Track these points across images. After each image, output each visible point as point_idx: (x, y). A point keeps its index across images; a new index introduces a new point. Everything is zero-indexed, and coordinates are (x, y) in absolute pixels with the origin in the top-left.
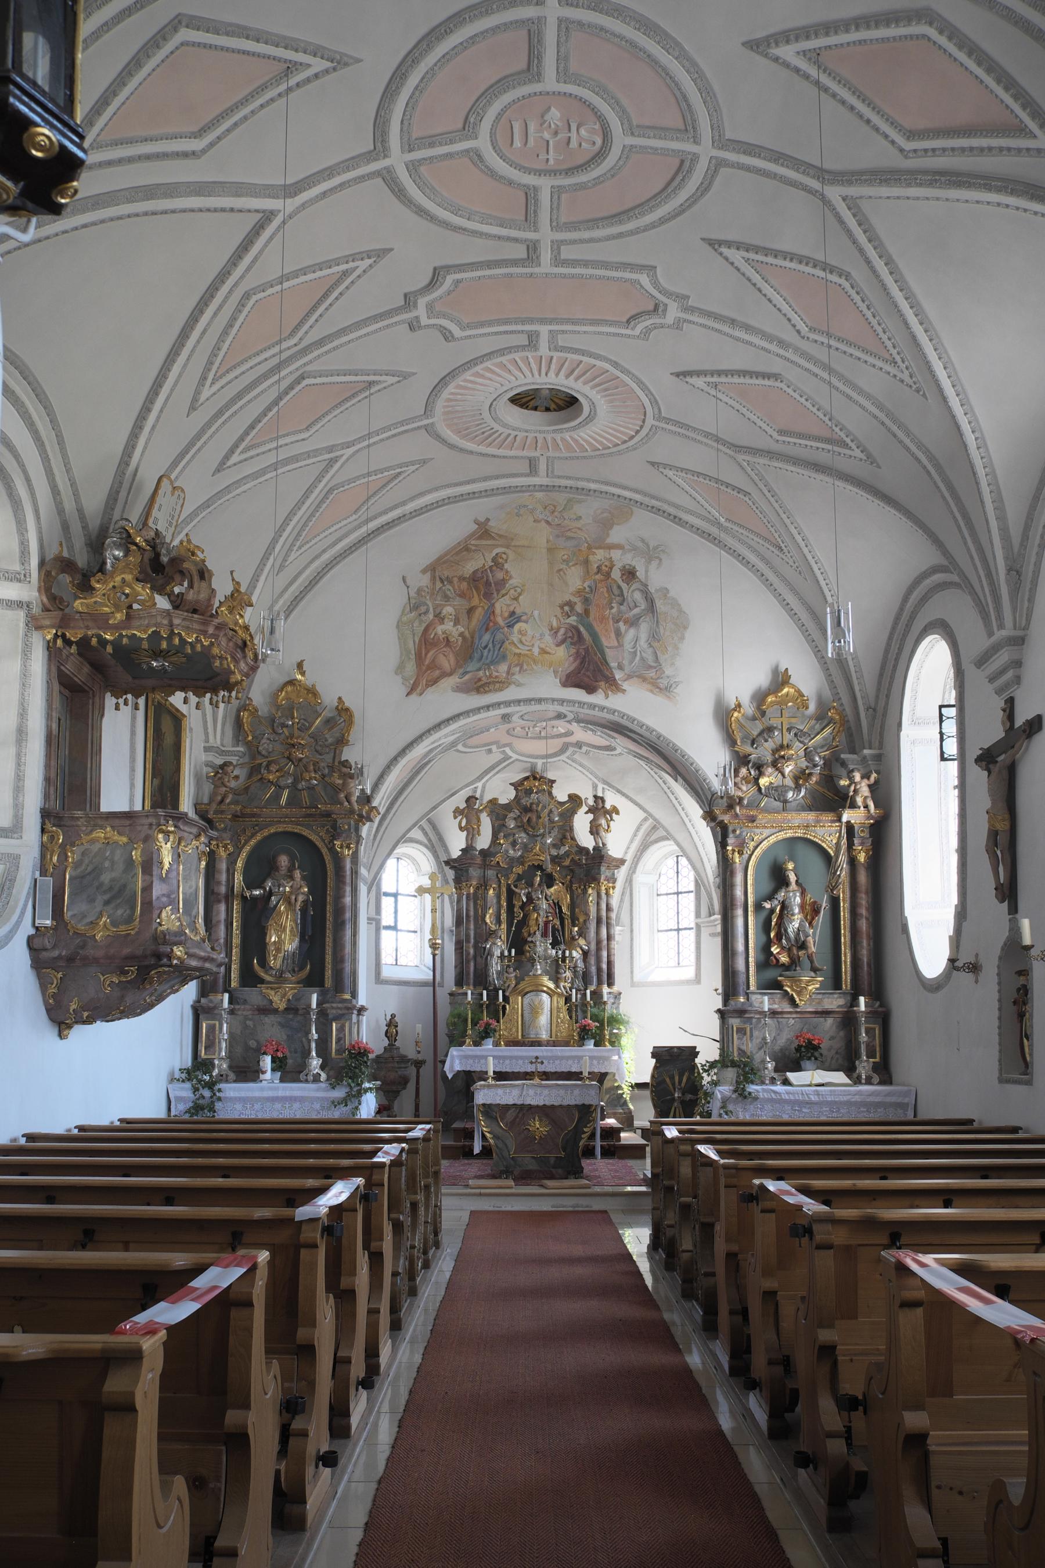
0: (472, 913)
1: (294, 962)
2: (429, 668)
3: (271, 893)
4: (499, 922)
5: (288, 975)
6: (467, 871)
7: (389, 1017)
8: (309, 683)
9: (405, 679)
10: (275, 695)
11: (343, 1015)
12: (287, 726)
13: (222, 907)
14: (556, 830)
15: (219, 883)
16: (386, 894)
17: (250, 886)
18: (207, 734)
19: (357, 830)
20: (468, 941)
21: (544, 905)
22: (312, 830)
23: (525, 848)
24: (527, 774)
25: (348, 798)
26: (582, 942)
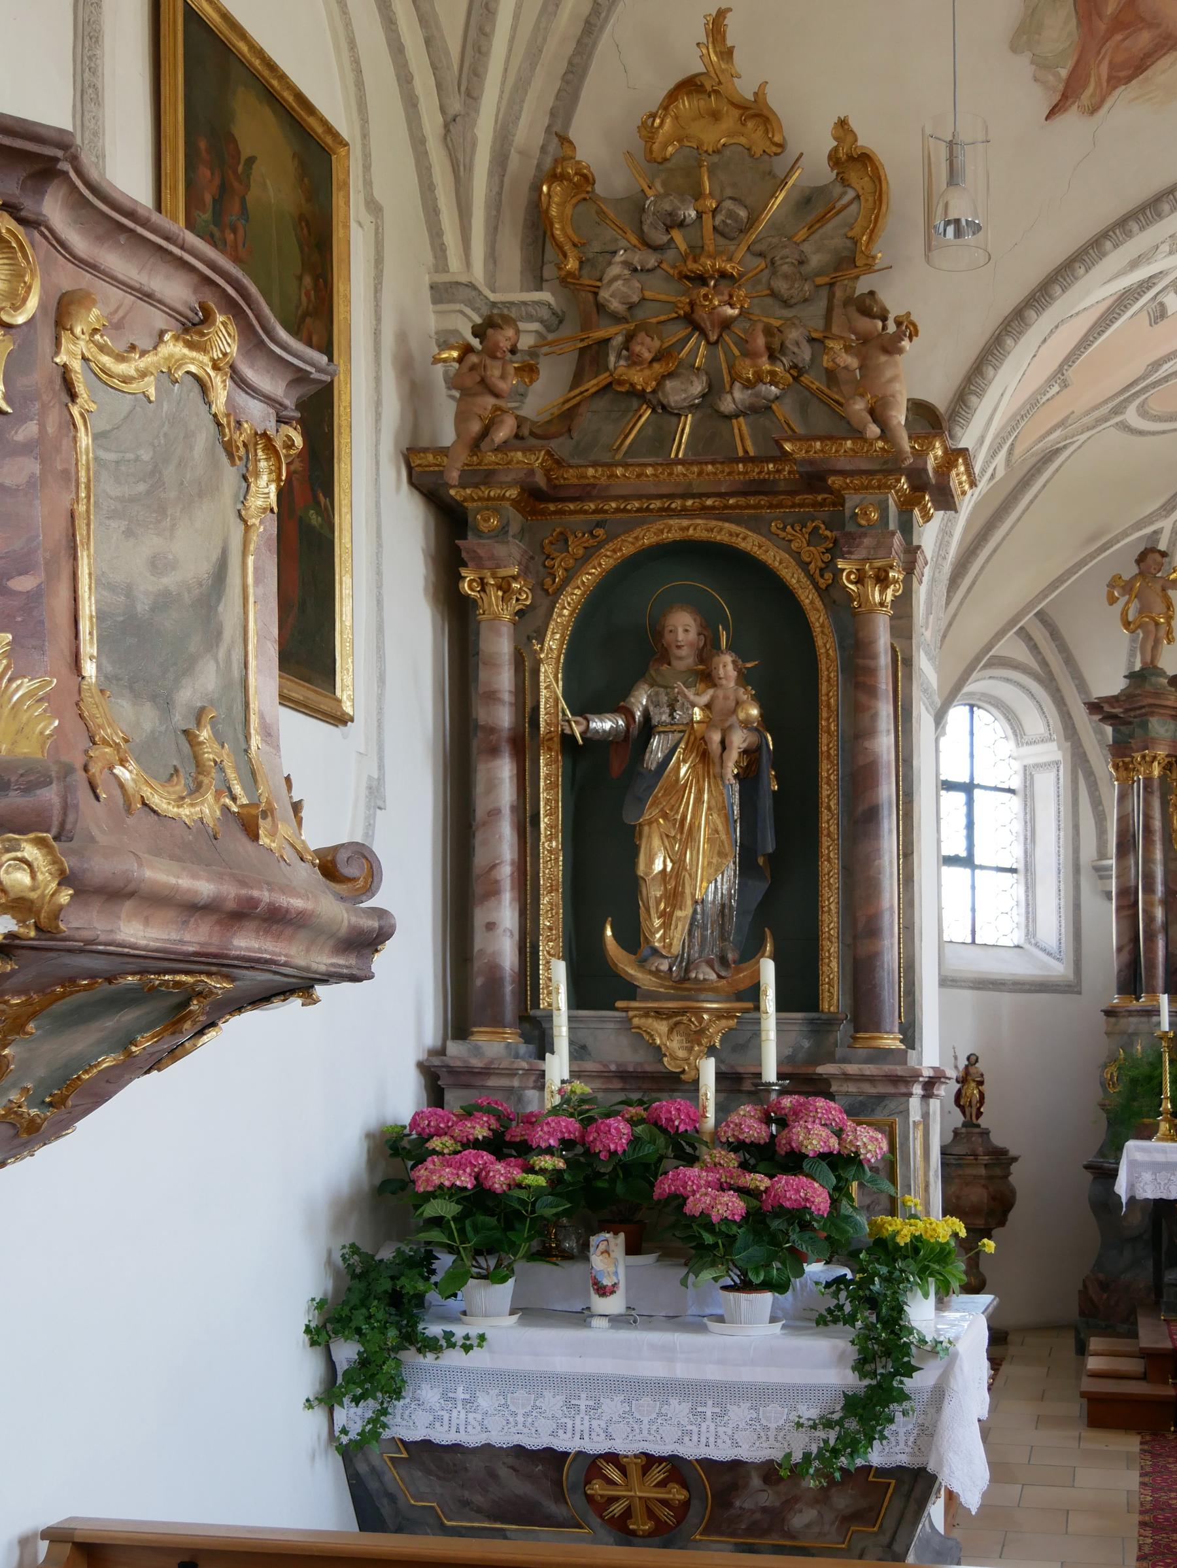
0: (1157, 824)
1: (723, 937)
2: (1119, 24)
3: (648, 728)
5: (707, 974)
6: (1144, 725)
8: (745, 89)
9: (1042, 65)
10: (648, 131)
11: (881, 1098)
12: (681, 225)
13: (505, 770)
15: (492, 697)
16: (949, 786)
17: (584, 706)
18: (439, 250)
19: (907, 528)
20: (1149, 889)
22: (770, 535)
25: (877, 414)
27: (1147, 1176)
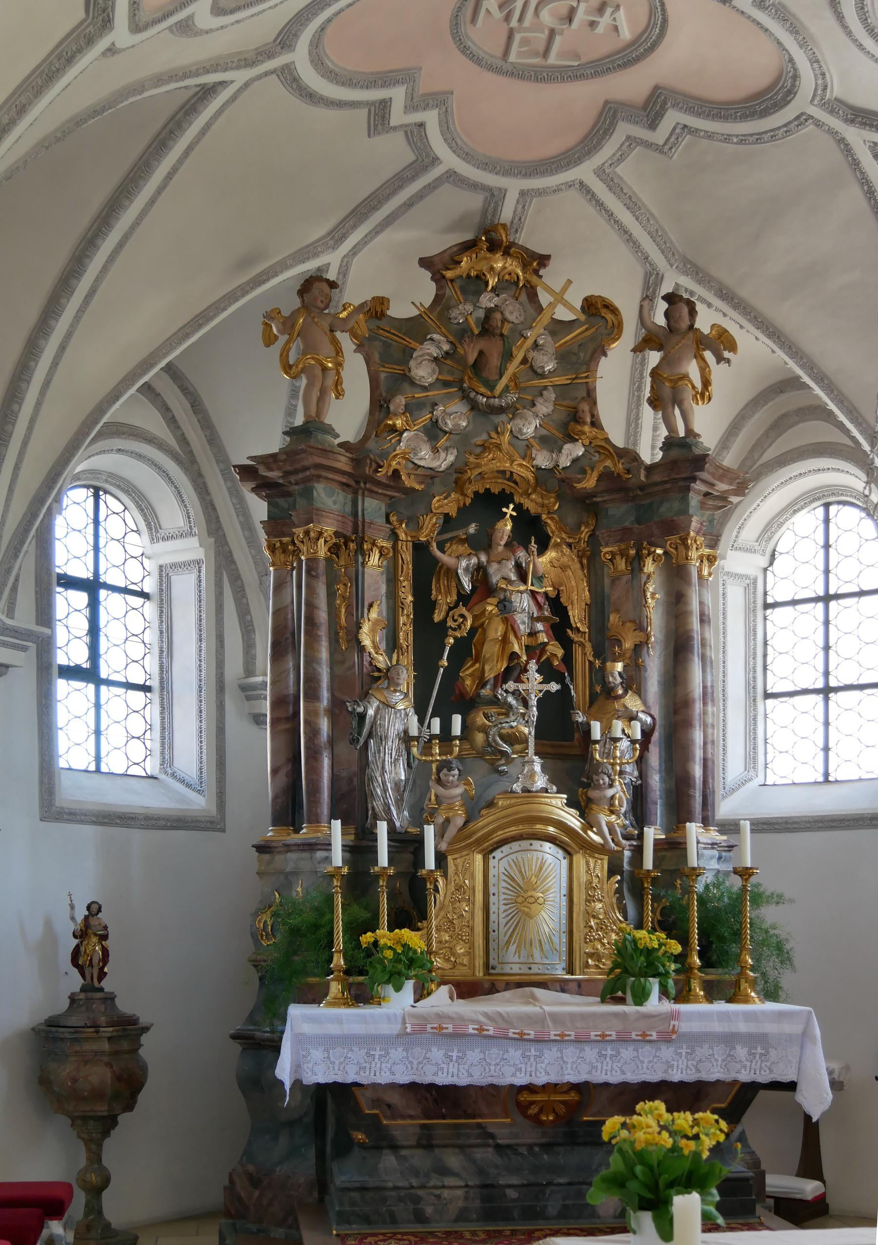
0: (322, 615)
4: (393, 645)
6: (308, 493)
7: (81, 913)
14: (551, 395)
20: (312, 695)
21: (523, 603)
23: (462, 440)
24: (469, 236)
26: (632, 702)
27: (317, 1054)
